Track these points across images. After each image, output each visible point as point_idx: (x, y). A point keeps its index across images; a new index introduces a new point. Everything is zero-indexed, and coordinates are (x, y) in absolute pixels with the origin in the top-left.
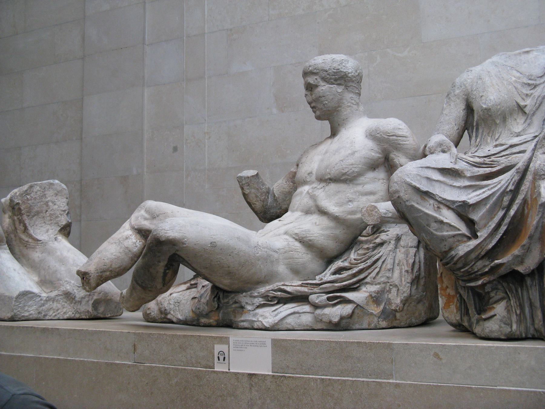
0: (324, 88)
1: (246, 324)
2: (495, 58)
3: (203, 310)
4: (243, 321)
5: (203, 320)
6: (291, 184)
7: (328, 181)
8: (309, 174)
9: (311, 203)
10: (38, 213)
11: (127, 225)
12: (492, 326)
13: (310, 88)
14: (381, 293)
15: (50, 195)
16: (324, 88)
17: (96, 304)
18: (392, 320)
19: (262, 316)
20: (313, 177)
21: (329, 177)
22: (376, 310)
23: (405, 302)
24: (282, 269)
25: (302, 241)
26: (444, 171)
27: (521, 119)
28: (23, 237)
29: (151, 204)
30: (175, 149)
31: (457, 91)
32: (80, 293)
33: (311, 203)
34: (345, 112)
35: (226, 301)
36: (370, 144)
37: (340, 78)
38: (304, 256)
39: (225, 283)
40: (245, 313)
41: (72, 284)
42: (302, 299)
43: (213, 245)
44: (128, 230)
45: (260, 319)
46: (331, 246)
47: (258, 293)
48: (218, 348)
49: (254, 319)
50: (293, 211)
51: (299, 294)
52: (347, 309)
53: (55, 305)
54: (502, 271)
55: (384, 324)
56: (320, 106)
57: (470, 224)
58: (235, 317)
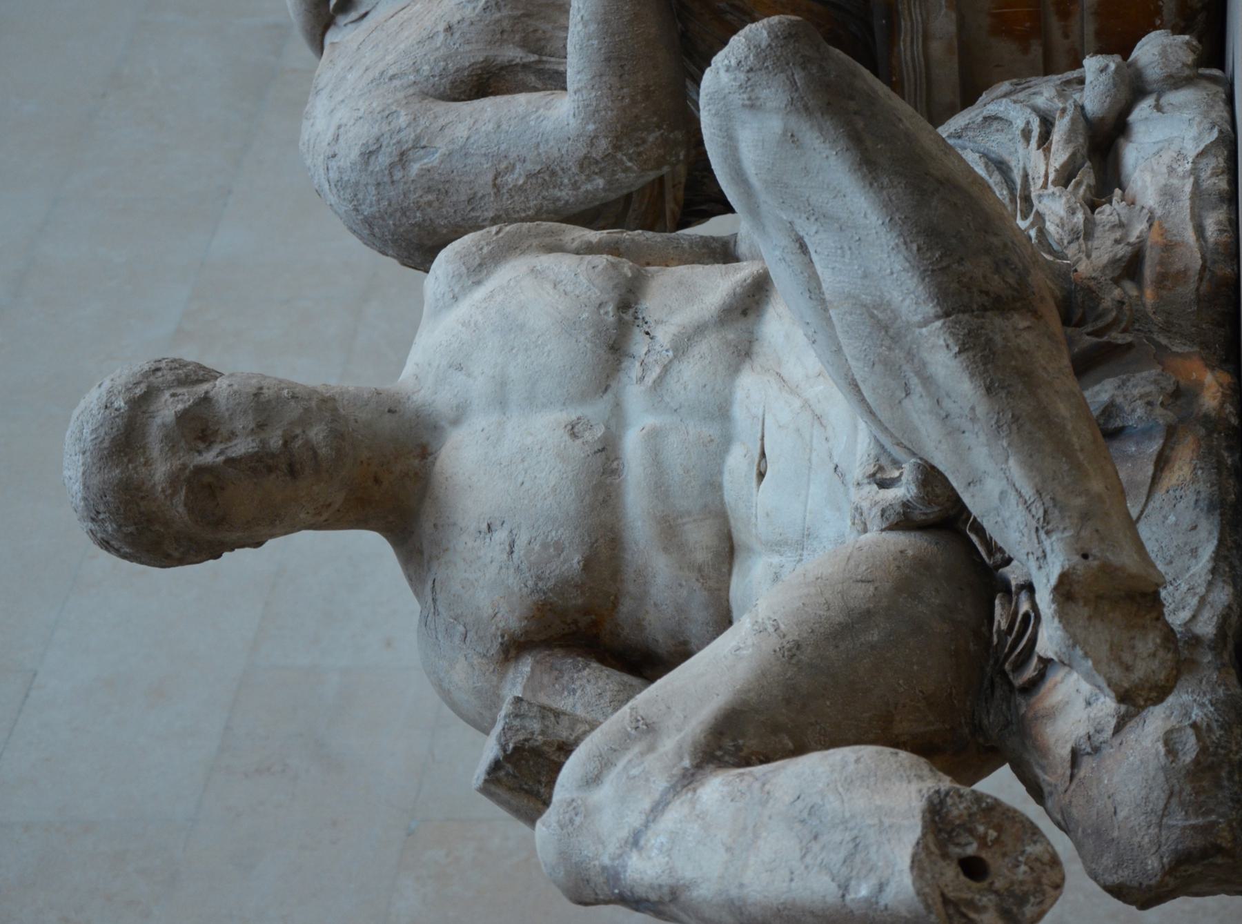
1: (1213, 222)
3: (1156, 382)
4: (1200, 230)
6: (586, 673)
7: (628, 317)
8: (574, 435)
9: (707, 346)
19: (1171, 170)
20: (595, 411)
21: (610, 308)
31: (403, 120)
33: (707, 346)
35: (1107, 302)
40: (1164, 232)
44: (693, 803)
45: (1189, 166)
47: (1073, 212)
49: (1188, 188)
50: (726, 441)
51: (1081, 140)
56: (294, 411)
58: (1183, 275)
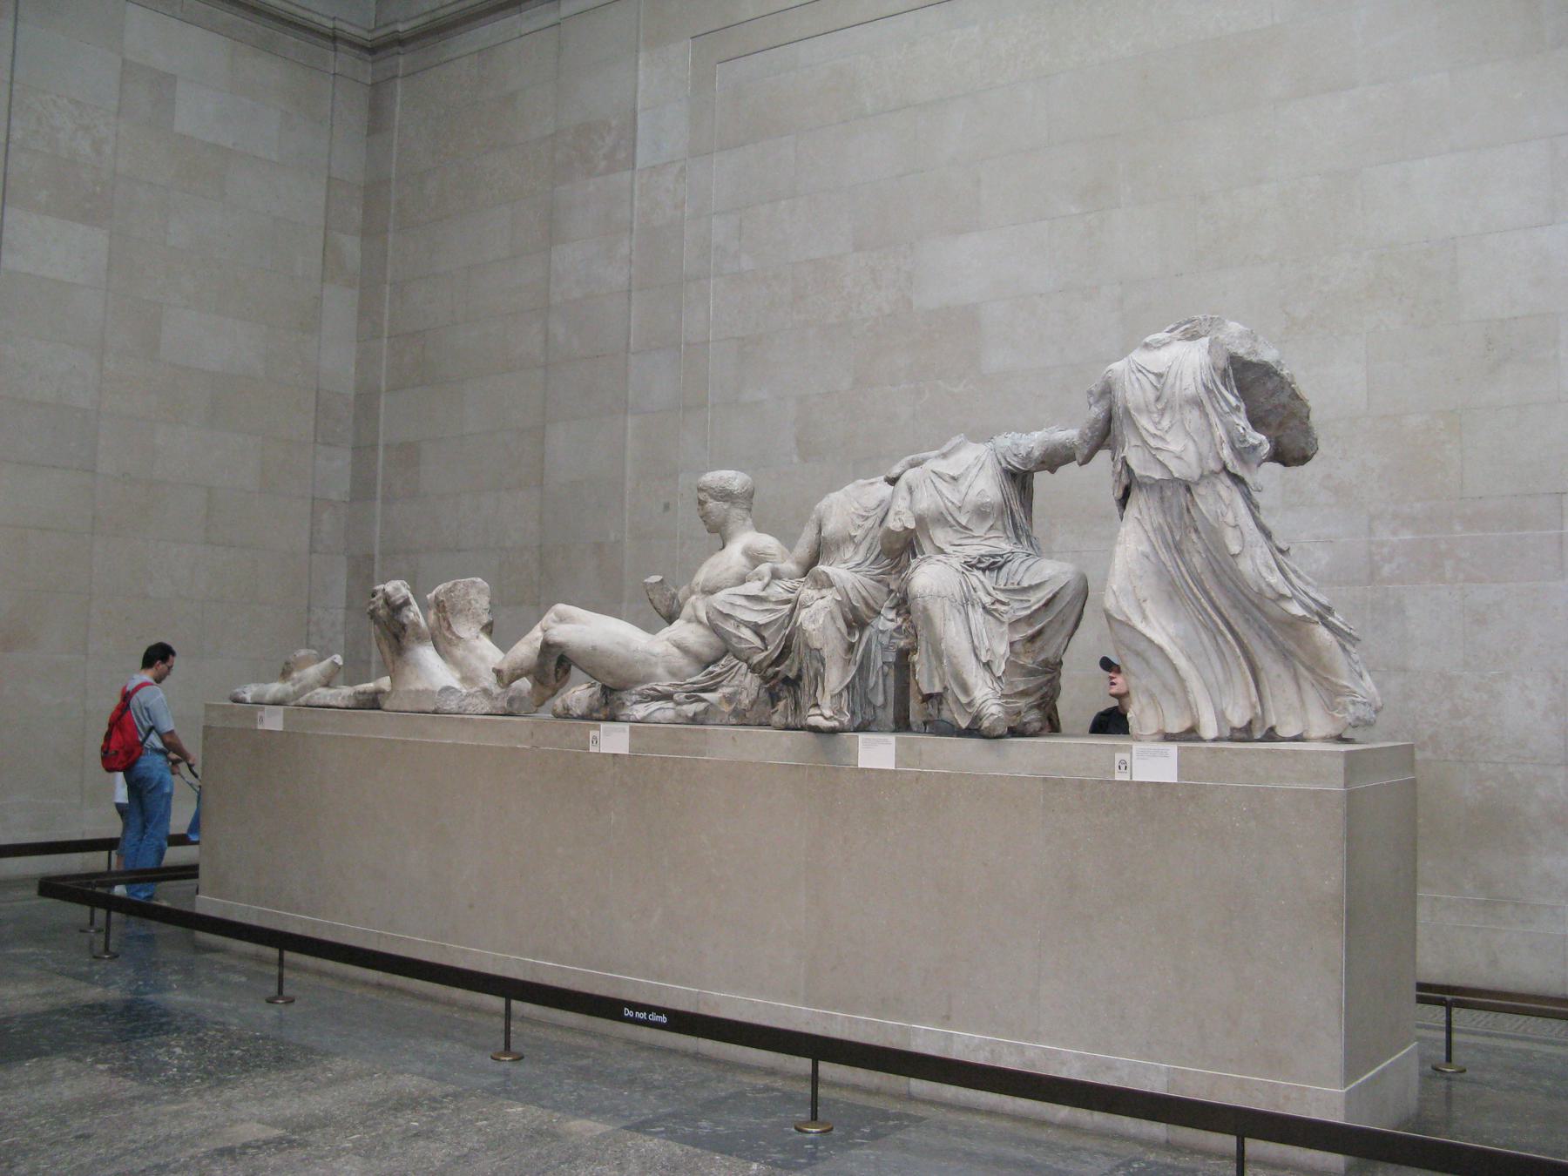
0: (712, 505)
2: (849, 488)
5: (595, 715)
10: (461, 611)
11: (538, 627)
12: (776, 718)
13: (702, 503)
14: (735, 693)
15: (473, 594)
16: (712, 505)
17: (511, 701)
18: (742, 718)
22: (726, 708)
23: (753, 703)
24: (660, 671)
25: (678, 647)
26: (748, 597)
27: (851, 548)
28: (447, 634)
29: (561, 607)
30: (667, 507)
32: (496, 690)
34: (731, 527)
36: (743, 560)
37: (726, 496)
38: (680, 661)
39: (609, 682)
41: (489, 681)
42: (667, 697)
43: (594, 648)
46: (707, 652)
48: (592, 733)
52: (700, 706)
53: (475, 701)
54: (780, 676)
55: (734, 721)
57: (763, 639)
